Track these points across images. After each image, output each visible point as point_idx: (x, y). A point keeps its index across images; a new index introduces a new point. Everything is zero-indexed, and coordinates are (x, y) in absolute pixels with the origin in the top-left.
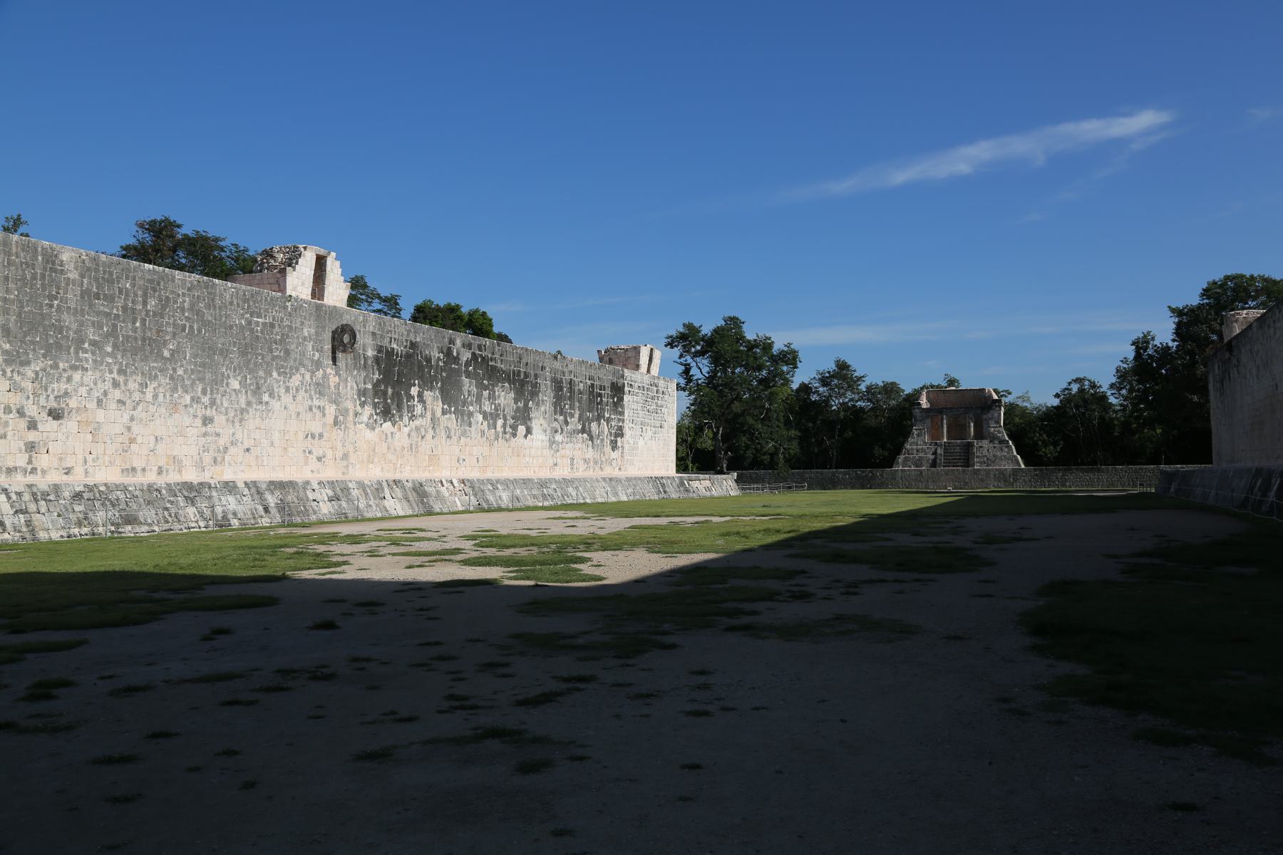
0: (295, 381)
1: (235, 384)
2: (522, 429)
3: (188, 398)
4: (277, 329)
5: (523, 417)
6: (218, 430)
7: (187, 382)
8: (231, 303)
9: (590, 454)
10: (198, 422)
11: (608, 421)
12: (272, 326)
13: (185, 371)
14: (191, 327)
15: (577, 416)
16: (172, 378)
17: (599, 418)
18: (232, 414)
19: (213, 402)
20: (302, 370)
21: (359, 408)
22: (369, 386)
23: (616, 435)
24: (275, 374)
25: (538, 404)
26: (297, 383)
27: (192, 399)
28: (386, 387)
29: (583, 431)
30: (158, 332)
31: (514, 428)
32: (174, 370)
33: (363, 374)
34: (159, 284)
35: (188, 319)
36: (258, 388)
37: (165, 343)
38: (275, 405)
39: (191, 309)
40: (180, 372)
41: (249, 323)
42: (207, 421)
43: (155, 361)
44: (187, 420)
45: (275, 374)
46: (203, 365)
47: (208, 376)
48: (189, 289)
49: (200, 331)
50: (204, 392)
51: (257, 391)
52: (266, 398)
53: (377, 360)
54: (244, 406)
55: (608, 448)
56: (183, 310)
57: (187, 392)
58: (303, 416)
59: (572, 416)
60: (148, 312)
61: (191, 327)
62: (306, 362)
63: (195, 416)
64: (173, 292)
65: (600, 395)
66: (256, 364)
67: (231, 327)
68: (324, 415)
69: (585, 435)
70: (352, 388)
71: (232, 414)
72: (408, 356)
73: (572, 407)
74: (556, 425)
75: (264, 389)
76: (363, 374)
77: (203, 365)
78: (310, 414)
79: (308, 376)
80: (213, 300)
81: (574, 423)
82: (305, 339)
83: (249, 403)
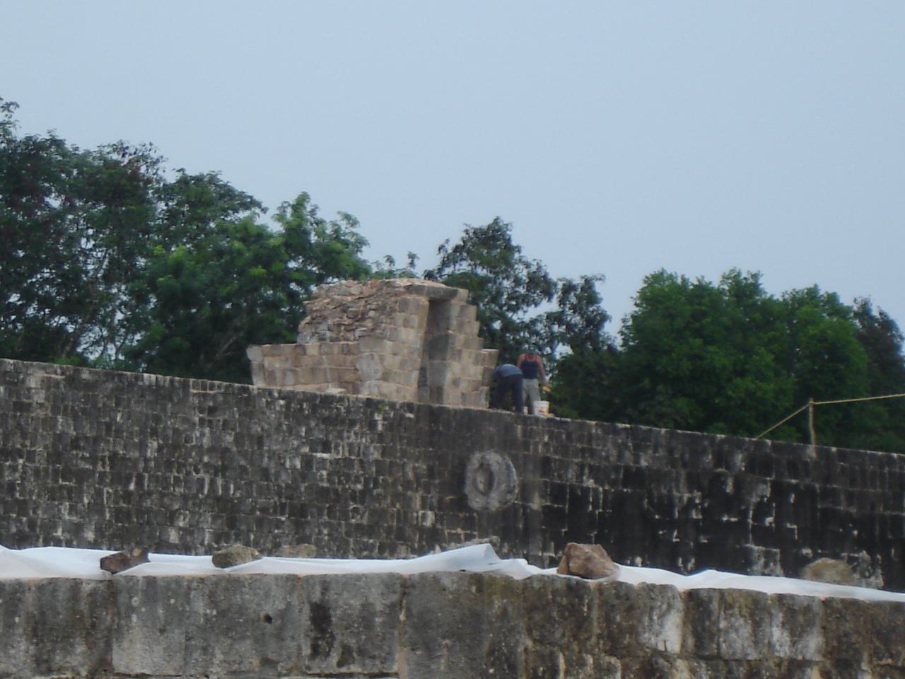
14: (212, 483)
60: (147, 460)
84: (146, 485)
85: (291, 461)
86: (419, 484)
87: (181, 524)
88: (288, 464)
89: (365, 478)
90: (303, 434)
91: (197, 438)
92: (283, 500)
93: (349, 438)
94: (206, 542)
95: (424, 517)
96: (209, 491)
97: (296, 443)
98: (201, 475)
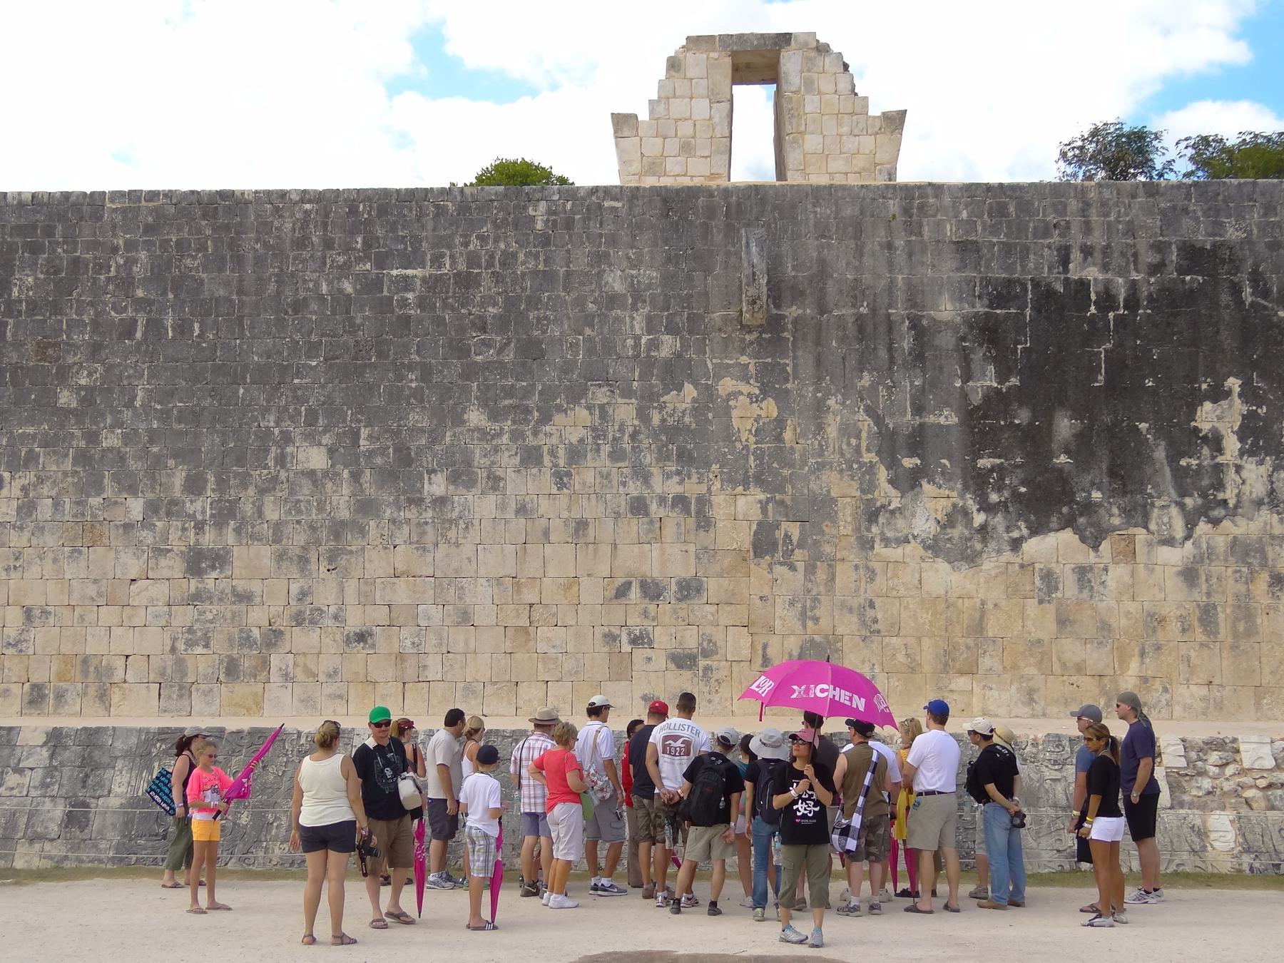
0: (572, 425)
1: (316, 458)
3: (136, 507)
4: (487, 285)
6: (241, 585)
7: (133, 465)
8: (302, 243)
10: (172, 566)
12: (466, 281)
13: (127, 439)
14: (155, 326)
16: (83, 458)
18: (297, 539)
19: (225, 513)
20: (601, 395)
21: (886, 492)
22: (948, 418)
24: (475, 417)
26: (574, 436)
27: (152, 508)
28: (1045, 415)
30: (41, 349)
32: (93, 438)
33: (909, 383)
34: (49, 232)
35: (143, 304)
36: (405, 458)
37: (63, 375)
38: (484, 506)
39: (158, 274)
40: (111, 440)
41: (371, 285)
42: (197, 562)
43: (31, 421)
44: (133, 565)
45: (475, 417)
46: (195, 416)
47: (209, 442)
48: (149, 229)
49: (183, 329)
50: (194, 486)
51: (402, 471)
52: (437, 486)
53: (988, 332)
54: (344, 514)
56: (125, 283)
57: (133, 490)
58: (605, 529)
61: (155, 326)
62: (615, 368)
63: (160, 552)
64: (95, 245)
66: (395, 396)
67: (299, 307)
68: (705, 522)
70: (849, 430)
71: (297, 539)
75: (428, 461)
76: (909, 383)
77: (195, 416)
78: (634, 526)
79: (625, 412)
80: (233, 245)
82: (613, 300)
83: (366, 507)
84: (9, 334)
85: (330, 283)
86: (638, 297)
87: (83, 382)
88: (324, 289)
89: (507, 299)
90: (359, 246)
91: (118, 267)
92: (314, 338)
93: (466, 244)
94: (138, 403)
95: (654, 345)
96: (145, 334)
97: (341, 259)
98: (130, 313)
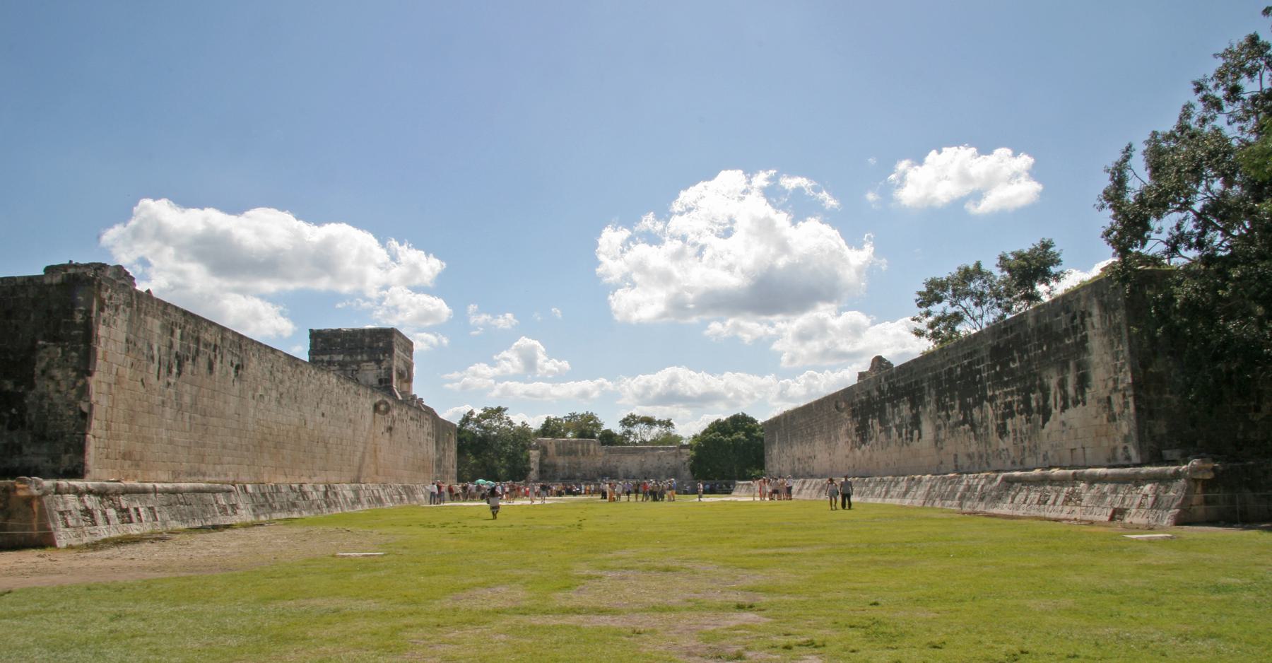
2: (916, 432)
5: (916, 422)
9: (974, 447)
11: (992, 399)
15: (957, 406)
17: (979, 403)
23: (1004, 417)
25: (925, 407)
29: (964, 422)
31: (912, 433)
55: (994, 437)
59: (952, 407)
65: (979, 372)
69: (967, 426)
72: (868, 401)
73: (952, 399)
74: (939, 422)
81: (957, 415)
